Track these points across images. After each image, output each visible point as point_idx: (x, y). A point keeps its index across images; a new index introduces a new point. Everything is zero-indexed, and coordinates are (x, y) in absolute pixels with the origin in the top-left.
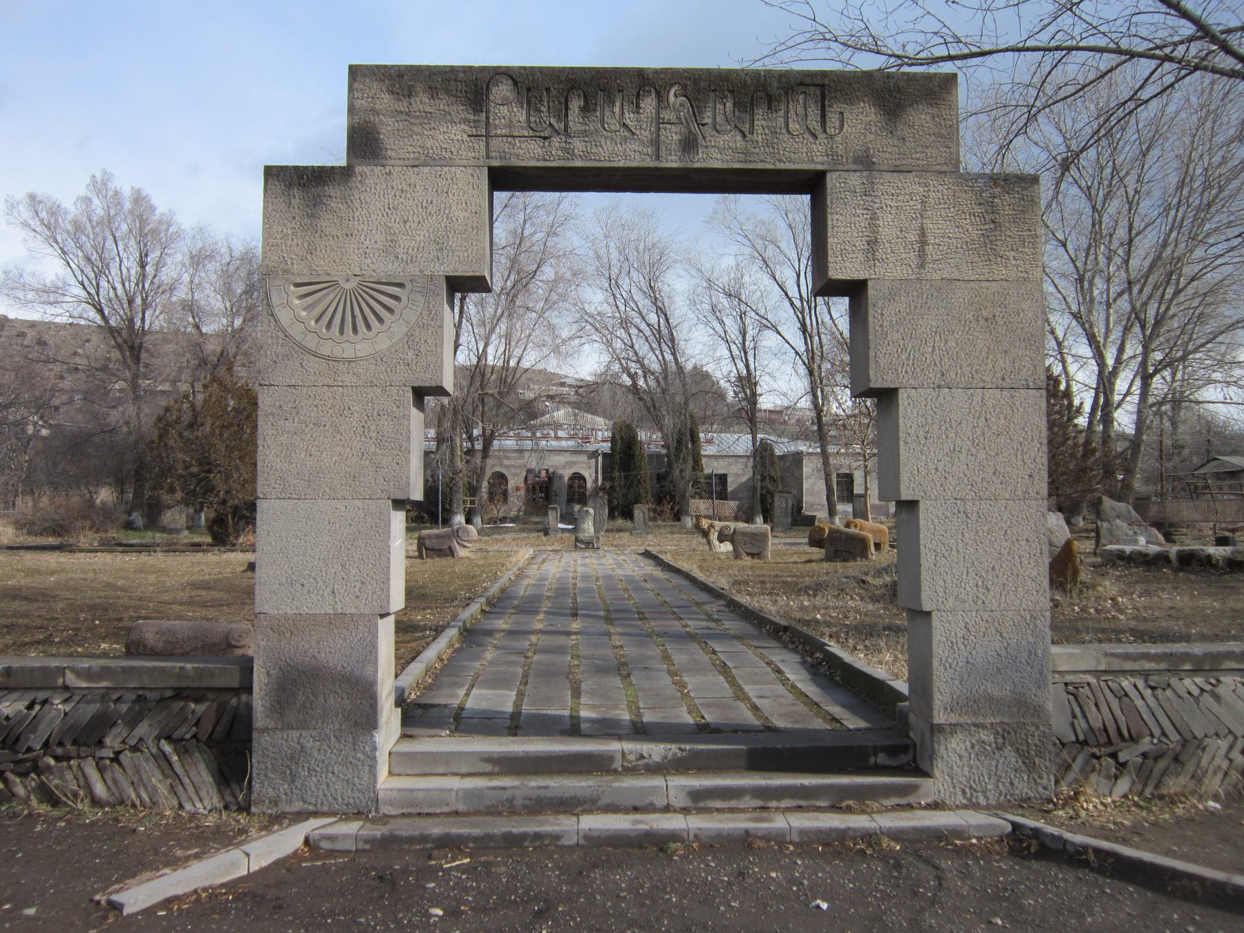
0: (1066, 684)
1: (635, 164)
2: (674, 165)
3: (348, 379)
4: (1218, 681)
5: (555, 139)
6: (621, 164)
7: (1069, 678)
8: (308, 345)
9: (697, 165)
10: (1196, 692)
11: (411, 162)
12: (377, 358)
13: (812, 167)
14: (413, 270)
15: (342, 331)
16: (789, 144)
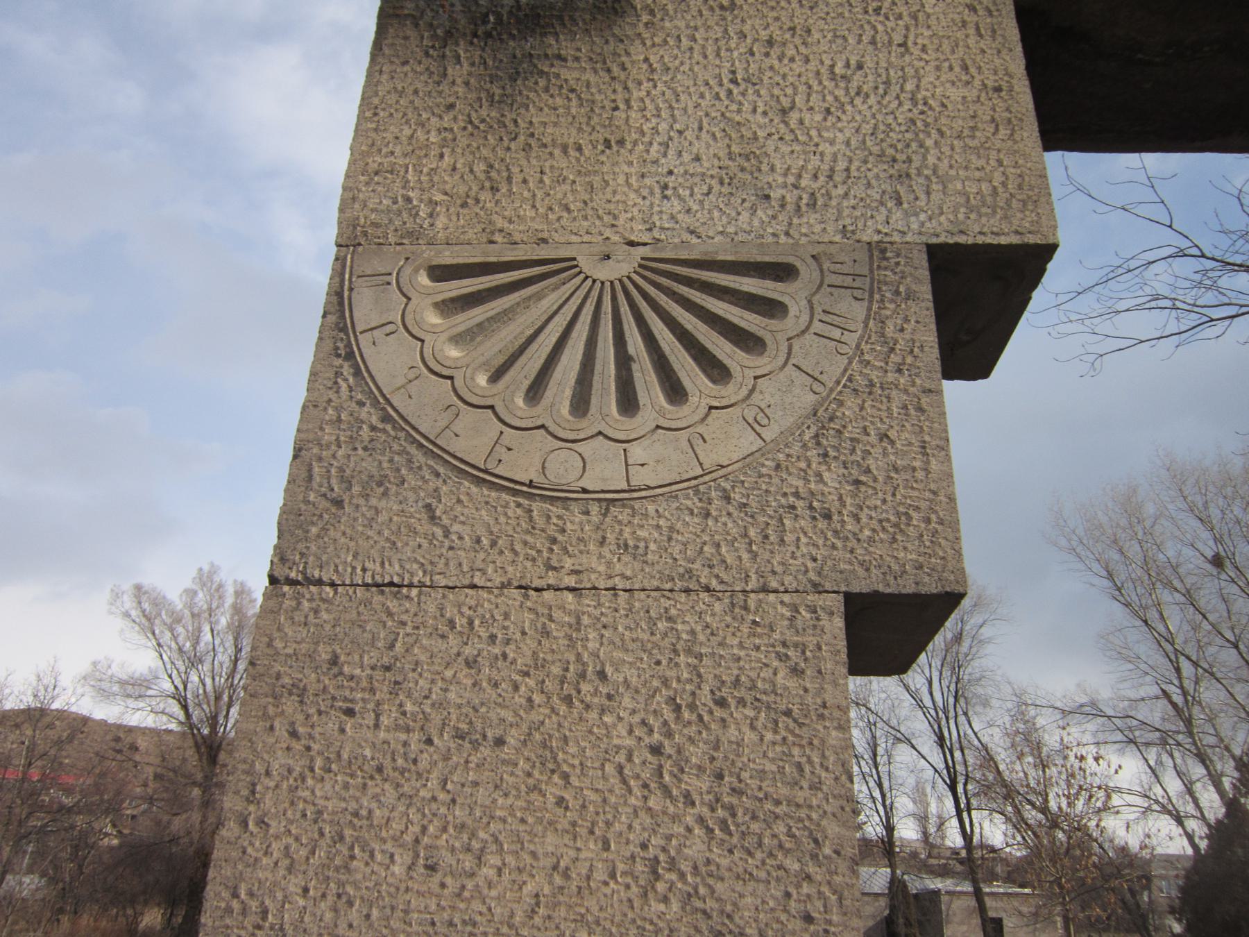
8: (459, 447)
12: (704, 489)
14: (817, 228)
15: (581, 404)
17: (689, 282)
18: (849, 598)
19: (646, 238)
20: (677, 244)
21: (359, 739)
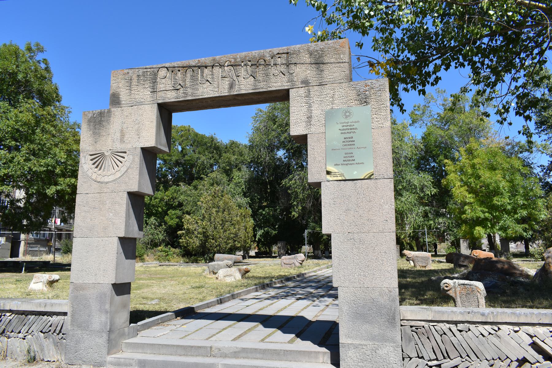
0: (411, 327)
1: (211, 96)
2: (226, 94)
3: (105, 190)
4: (499, 329)
5: (182, 89)
6: (206, 97)
7: (413, 323)
9: (235, 93)
10: (486, 334)
13: (283, 88)
14: (129, 146)
20: (115, 149)
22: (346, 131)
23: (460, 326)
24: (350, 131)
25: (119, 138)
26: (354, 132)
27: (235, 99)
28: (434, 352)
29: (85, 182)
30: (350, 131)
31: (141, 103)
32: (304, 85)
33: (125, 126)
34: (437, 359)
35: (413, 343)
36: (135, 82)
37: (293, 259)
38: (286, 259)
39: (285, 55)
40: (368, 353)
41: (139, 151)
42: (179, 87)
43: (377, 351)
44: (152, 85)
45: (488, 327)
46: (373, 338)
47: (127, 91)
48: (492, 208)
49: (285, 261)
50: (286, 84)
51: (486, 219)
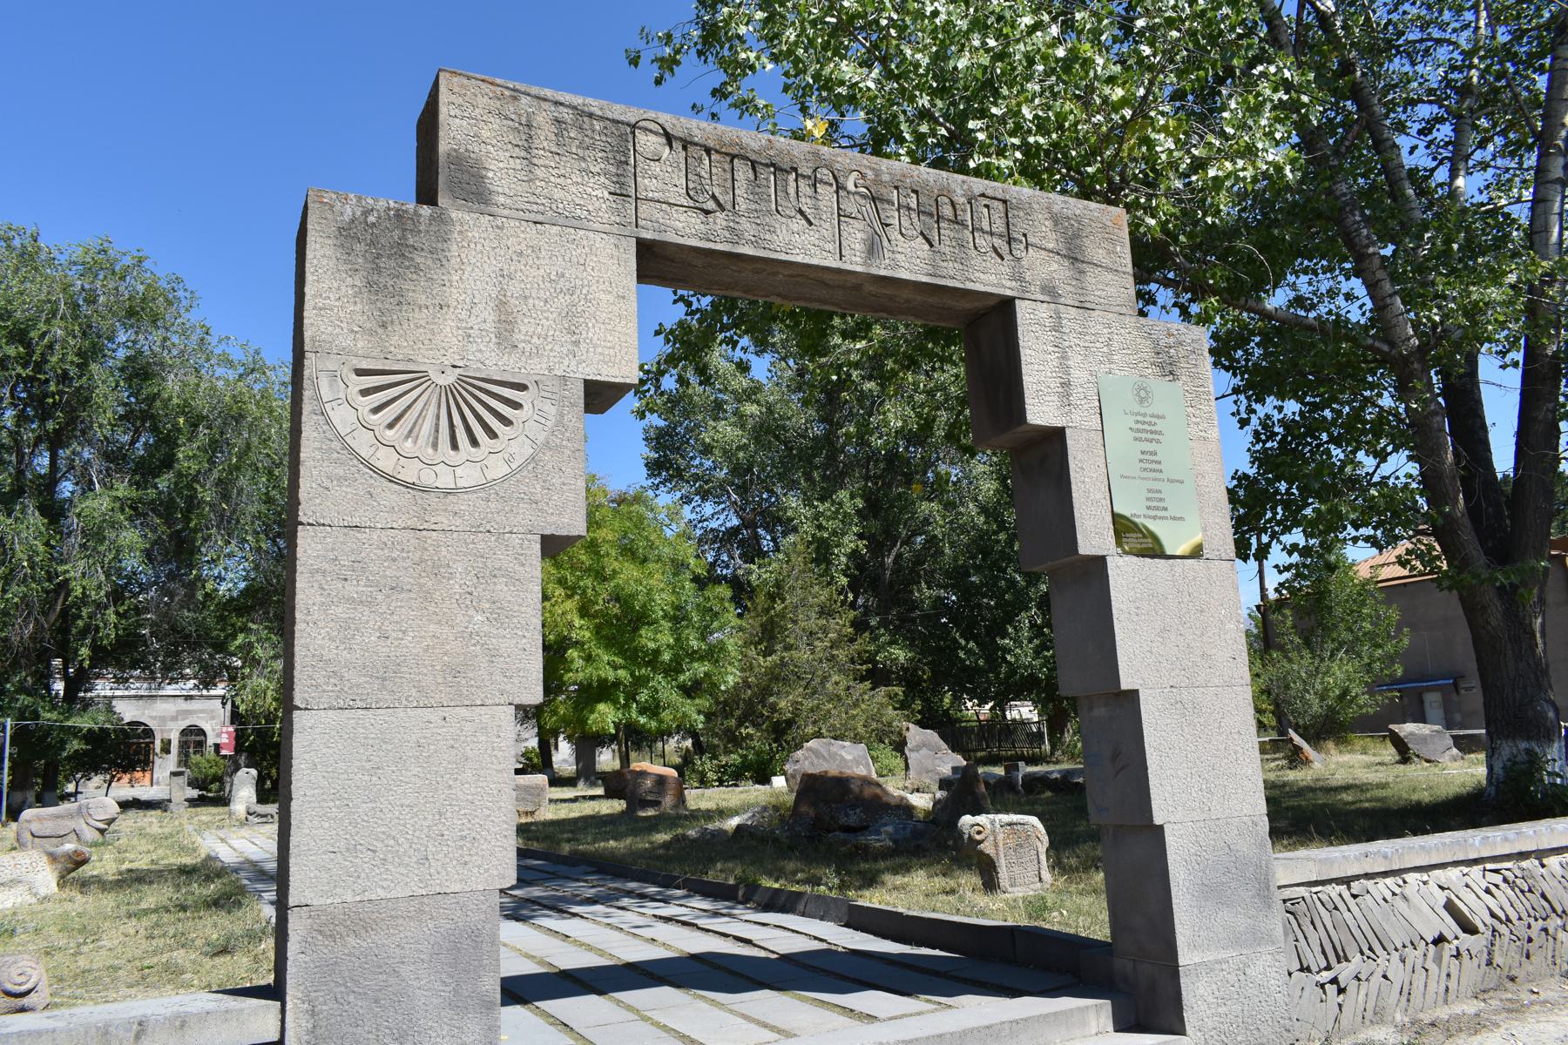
0: (1285, 901)
1: (815, 261)
2: (859, 269)
3: (444, 521)
6: (799, 259)
9: (883, 273)
10: (1389, 896)
11: (533, 217)
16: (977, 261)
17: (480, 389)
18: (543, 537)
19: (460, 364)
21: (351, 589)
22: (1144, 436)
23: (1356, 887)
24: (1150, 436)
25: (490, 326)
26: (1158, 442)
27: (857, 287)
28: (1324, 952)
29: (341, 479)
30: (1150, 436)
31: (575, 223)
32: (1047, 298)
33: (514, 288)
34: (1328, 968)
35: (1292, 937)
36: (545, 135)
37: (71, 816)
38: (40, 819)
39: (1001, 206)
40: (1232, 978)
41: (579, 392)
42: (711, 205)
43: (1248, 971)
44: (613, 169)
45: (1389, 881)
46: (1236, 941)
47: (518, 164)
48: (633, 656)
49: (35, 827)
50: (1008, 284)
51: (617, 684)
